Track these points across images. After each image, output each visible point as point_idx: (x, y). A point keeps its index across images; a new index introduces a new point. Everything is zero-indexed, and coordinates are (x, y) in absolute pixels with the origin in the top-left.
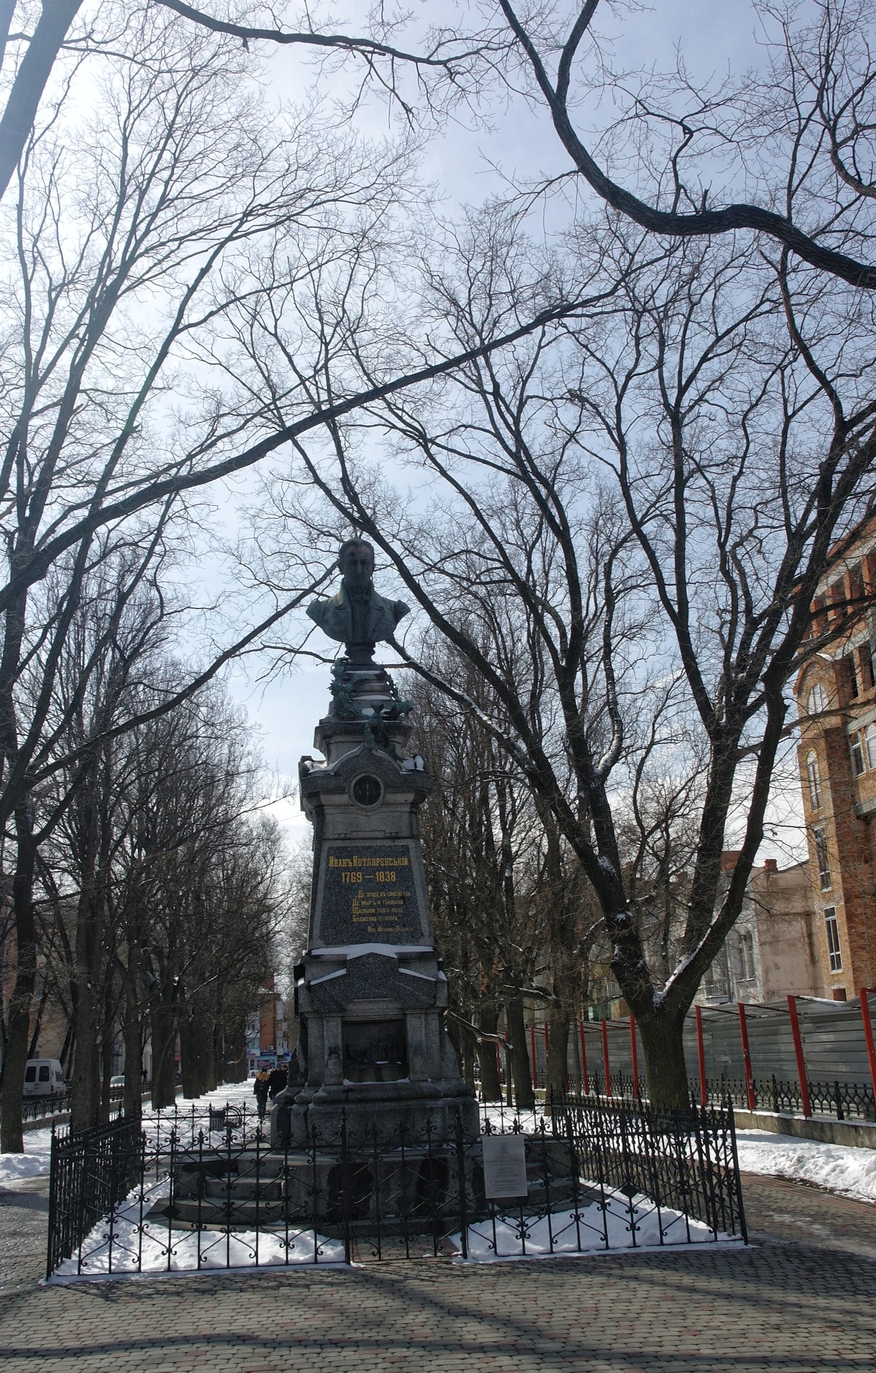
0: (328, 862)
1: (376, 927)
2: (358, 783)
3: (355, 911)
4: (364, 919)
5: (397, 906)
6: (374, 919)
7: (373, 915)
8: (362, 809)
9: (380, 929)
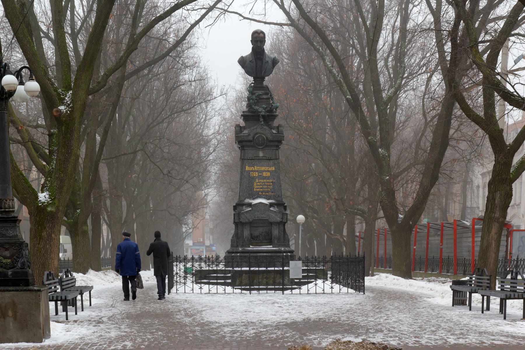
1: (262, 193)
3: (255, 187)
5: (270, 185)
6: (262, 190)
7: (261, 188)
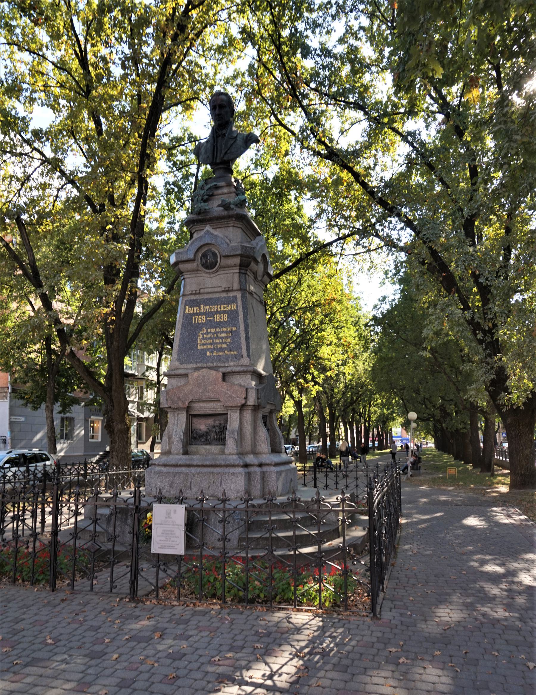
0: (185, 310)
1: (212, 352)
2: (203, 255)
3: (200, 342)
4: (205, 347)
5: (227, 337)
6: (211, 347)
7: (211, 344)
8: (207, 273)
9: (215, 353)
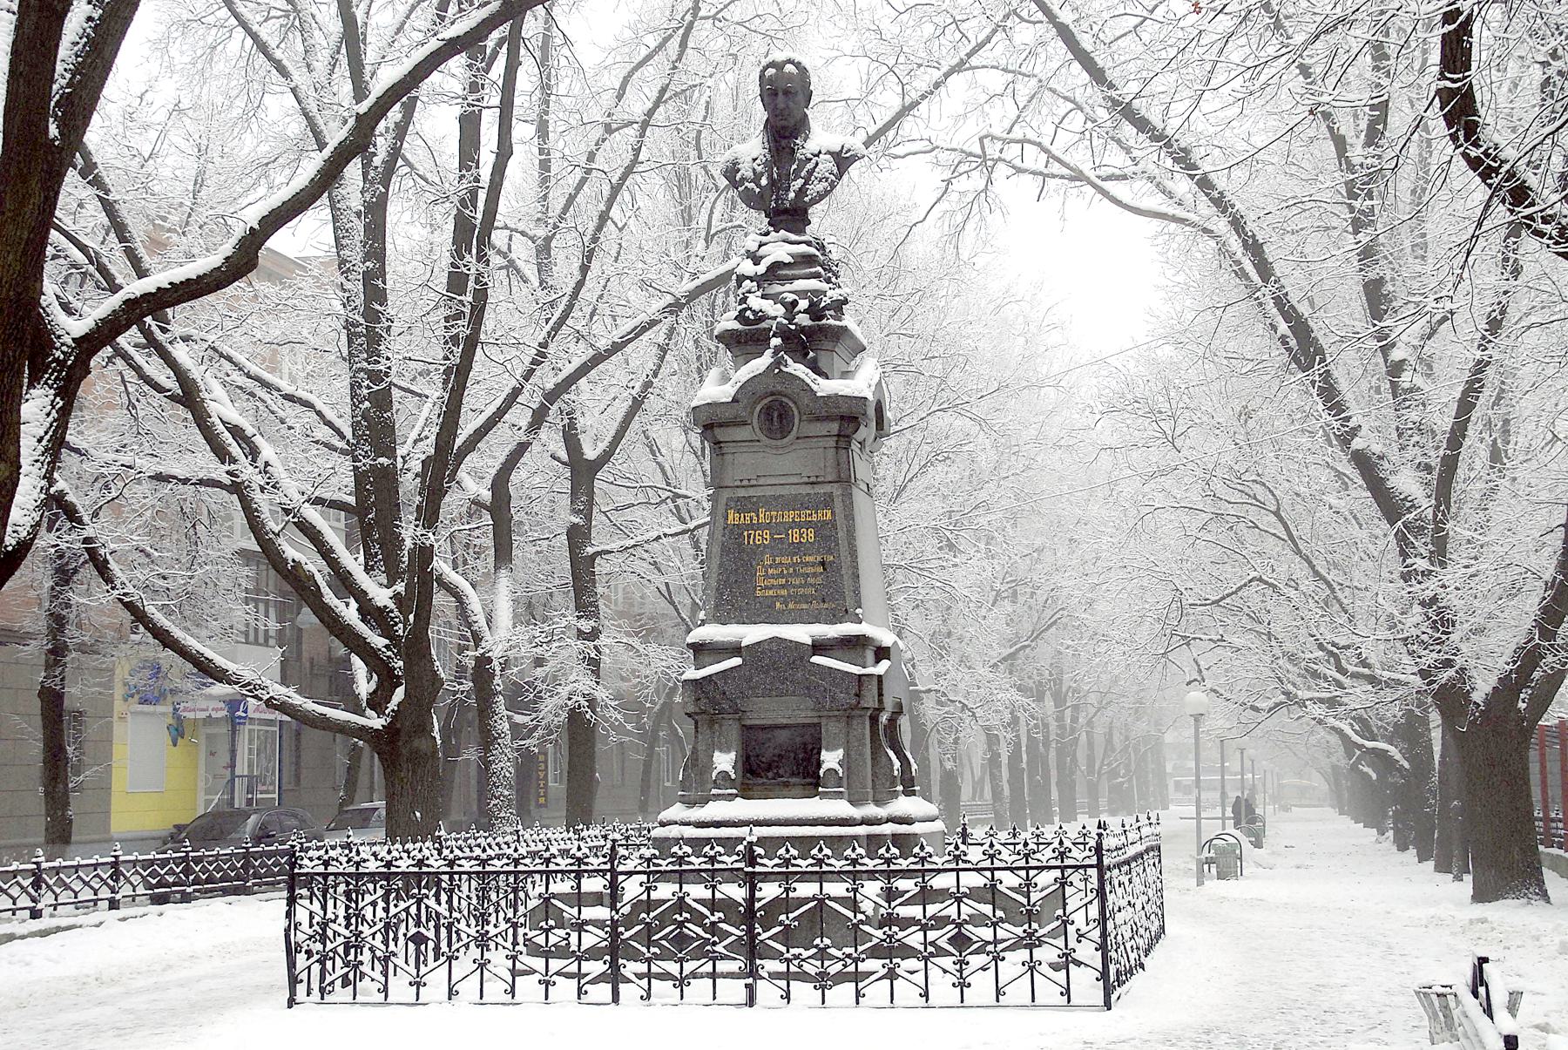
1: (785, 603)
5: (815, 575)
7: (783, 586)
9: (791, 606)
